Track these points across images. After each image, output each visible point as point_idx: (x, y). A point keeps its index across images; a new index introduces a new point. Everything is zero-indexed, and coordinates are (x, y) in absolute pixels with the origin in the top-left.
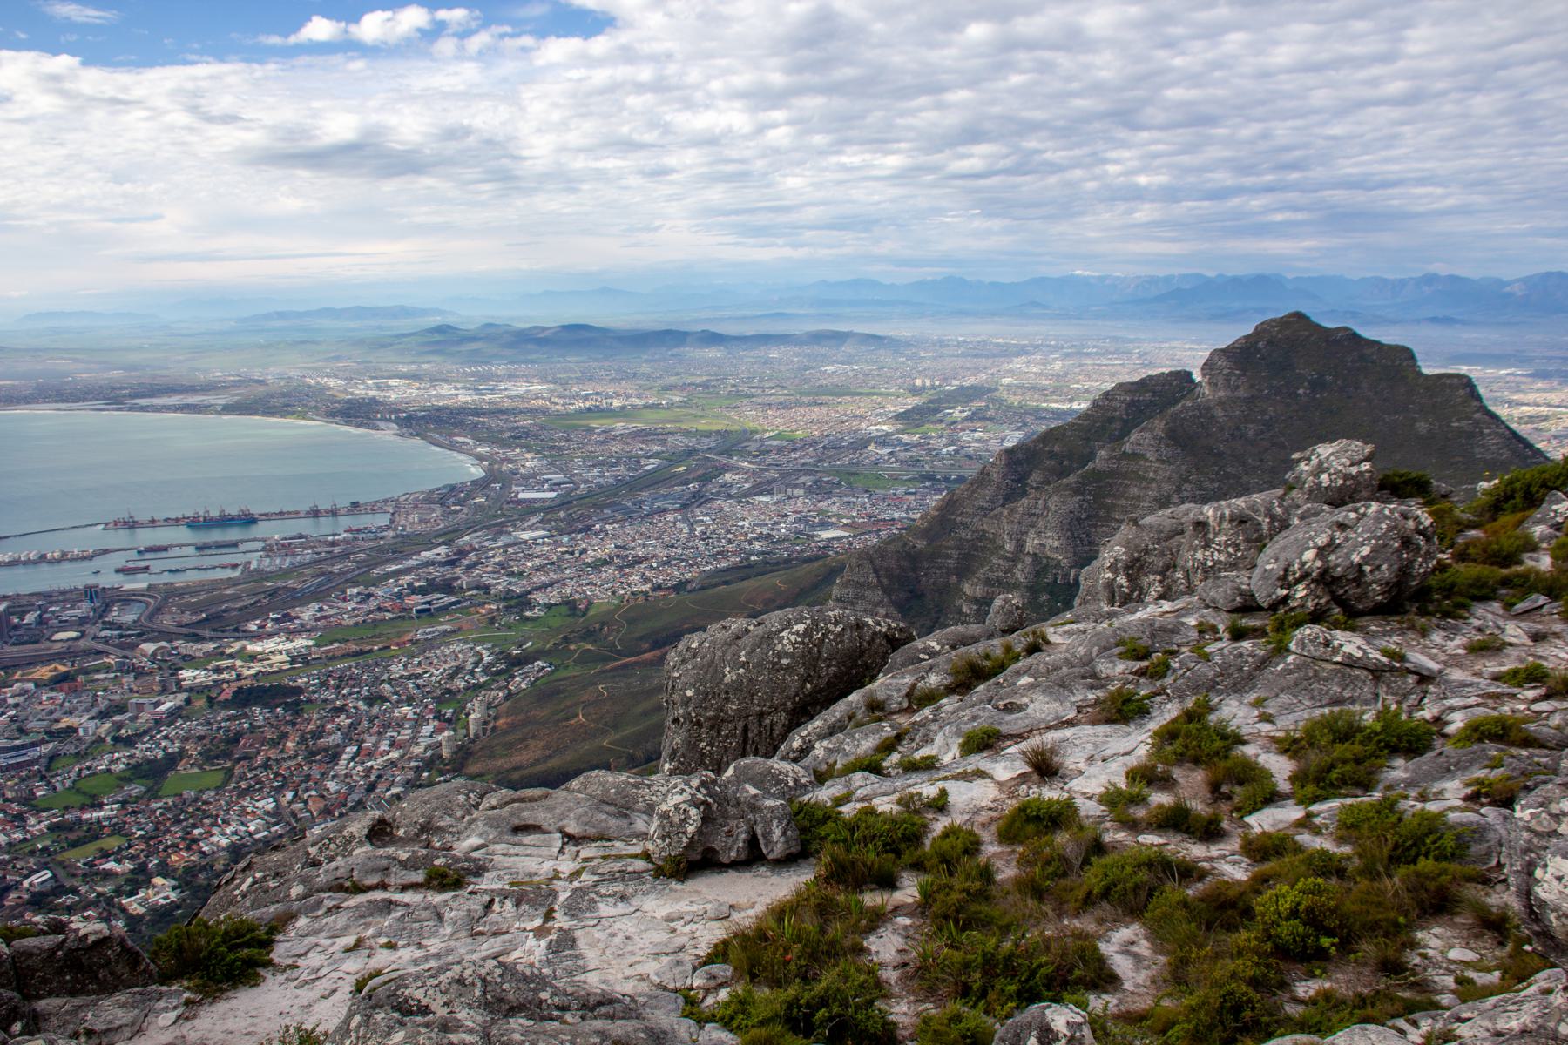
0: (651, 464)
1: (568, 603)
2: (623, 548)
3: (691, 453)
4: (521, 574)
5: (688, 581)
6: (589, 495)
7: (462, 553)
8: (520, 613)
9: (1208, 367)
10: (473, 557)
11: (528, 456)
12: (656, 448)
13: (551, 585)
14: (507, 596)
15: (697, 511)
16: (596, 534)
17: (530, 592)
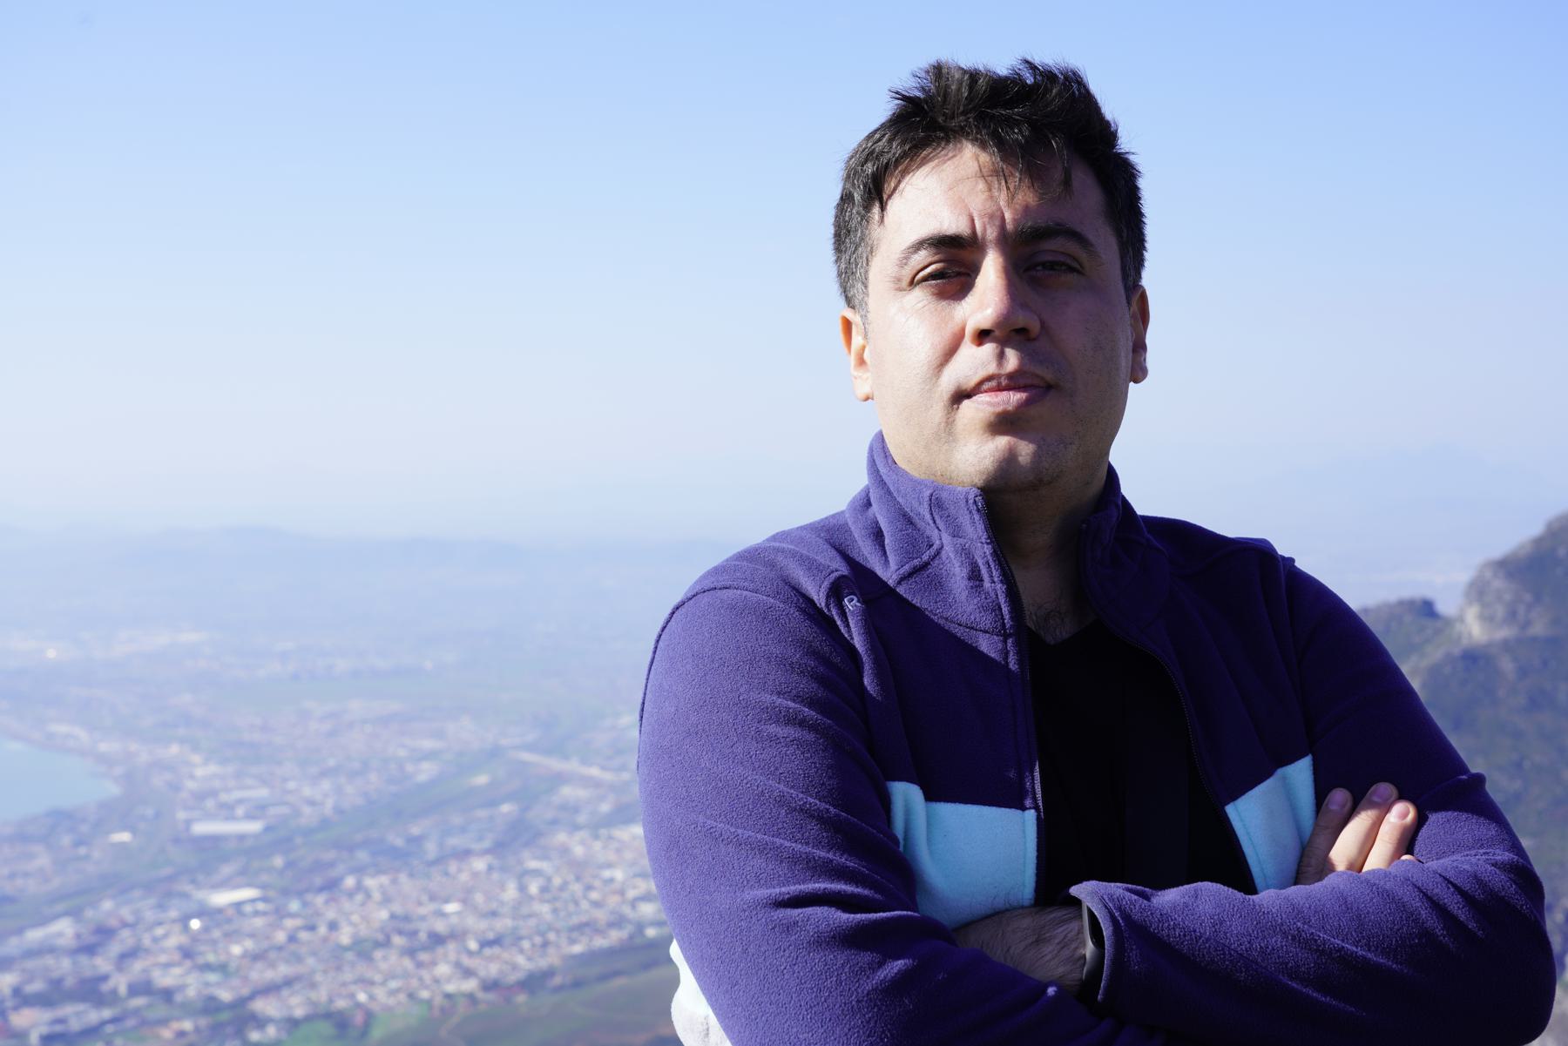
0: (426, 771)
1: (328, 1016)
2: (407, 918)
3: (495, 753)
4: (222, 968)
5: (549, 973)
6: (325, 824)
7: (105, 933)
8: (240, 1033)
9: (1477, 591)
10: (126, 938)
11: (196, 758)
12: (428, 744)
13: (288, 982)
14: (210, 1006)
15: (526, 854)
16: (351, 894)
17: (253, 996)
